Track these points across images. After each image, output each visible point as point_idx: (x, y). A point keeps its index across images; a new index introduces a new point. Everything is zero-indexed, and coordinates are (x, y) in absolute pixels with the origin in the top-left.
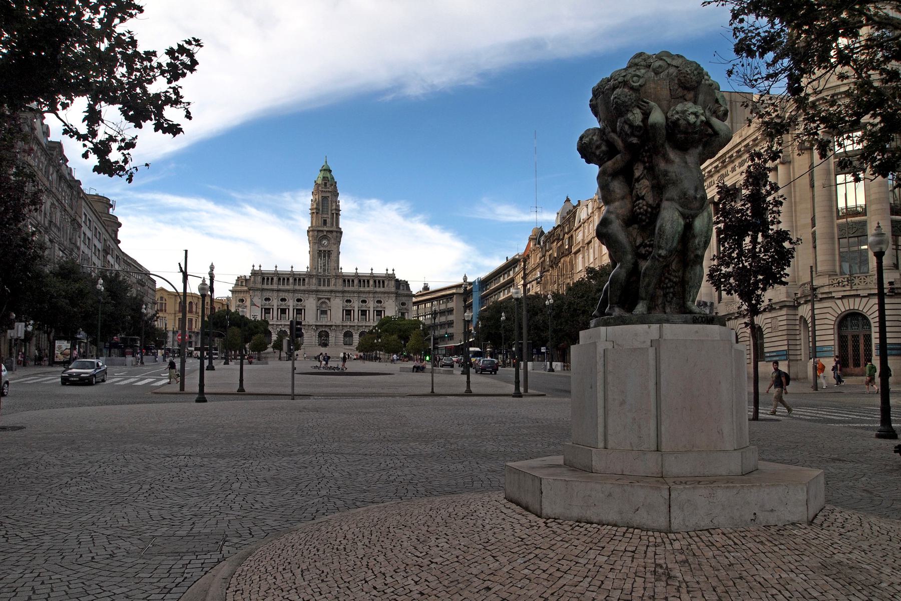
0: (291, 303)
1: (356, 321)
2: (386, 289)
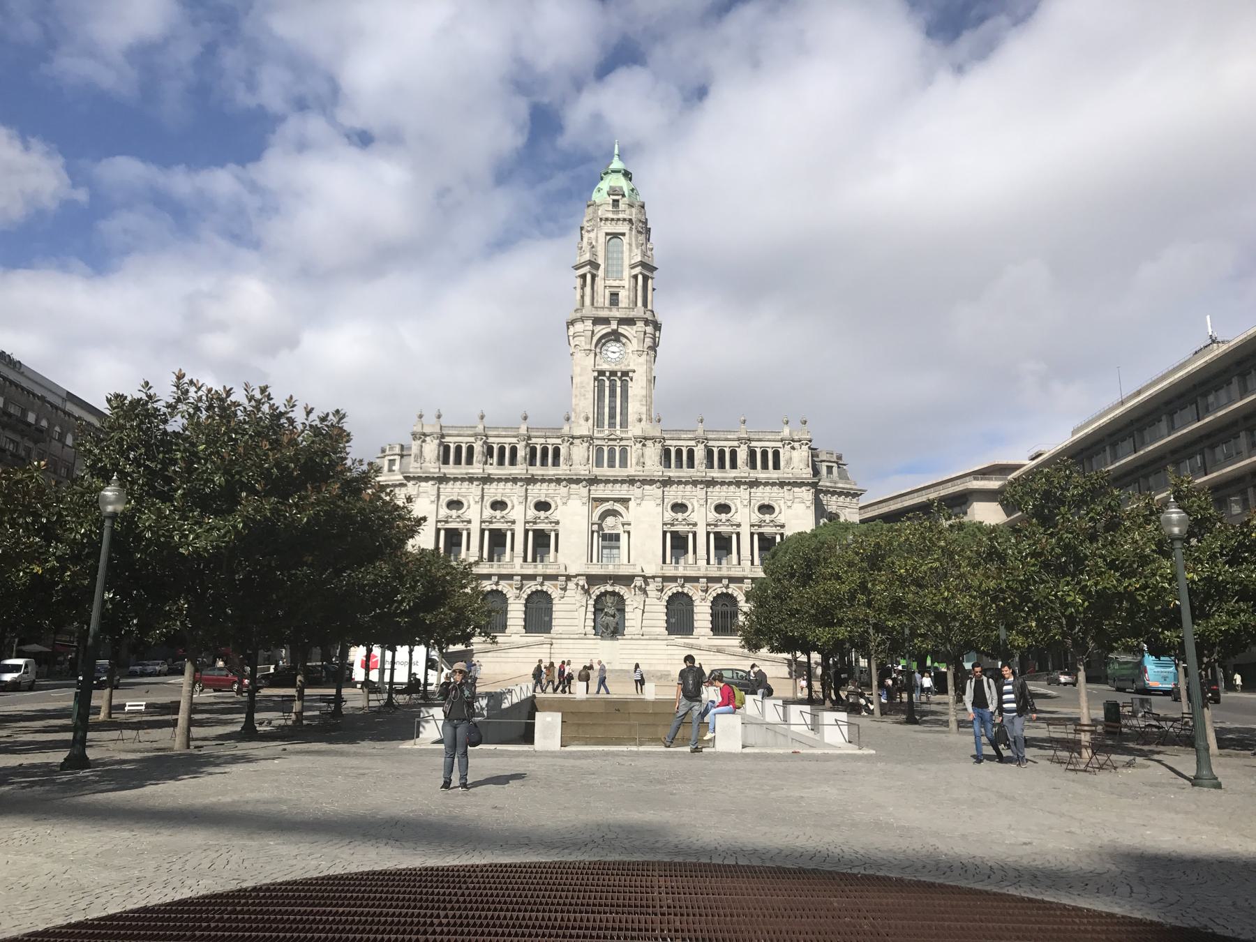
0: (519, 514)
2: (784, 473)
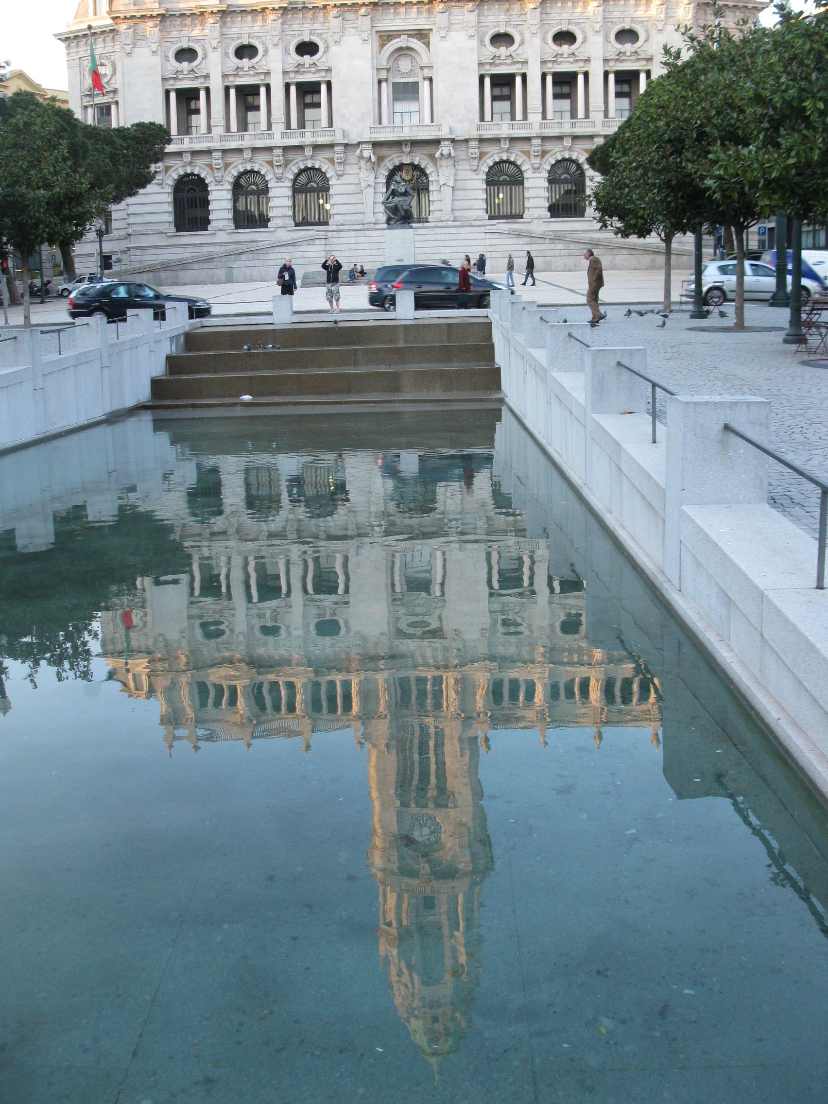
1: (535, 118)
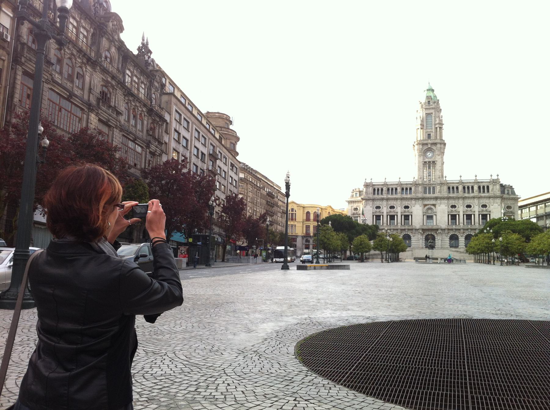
0: (399, 210)
2: (491, 193)
